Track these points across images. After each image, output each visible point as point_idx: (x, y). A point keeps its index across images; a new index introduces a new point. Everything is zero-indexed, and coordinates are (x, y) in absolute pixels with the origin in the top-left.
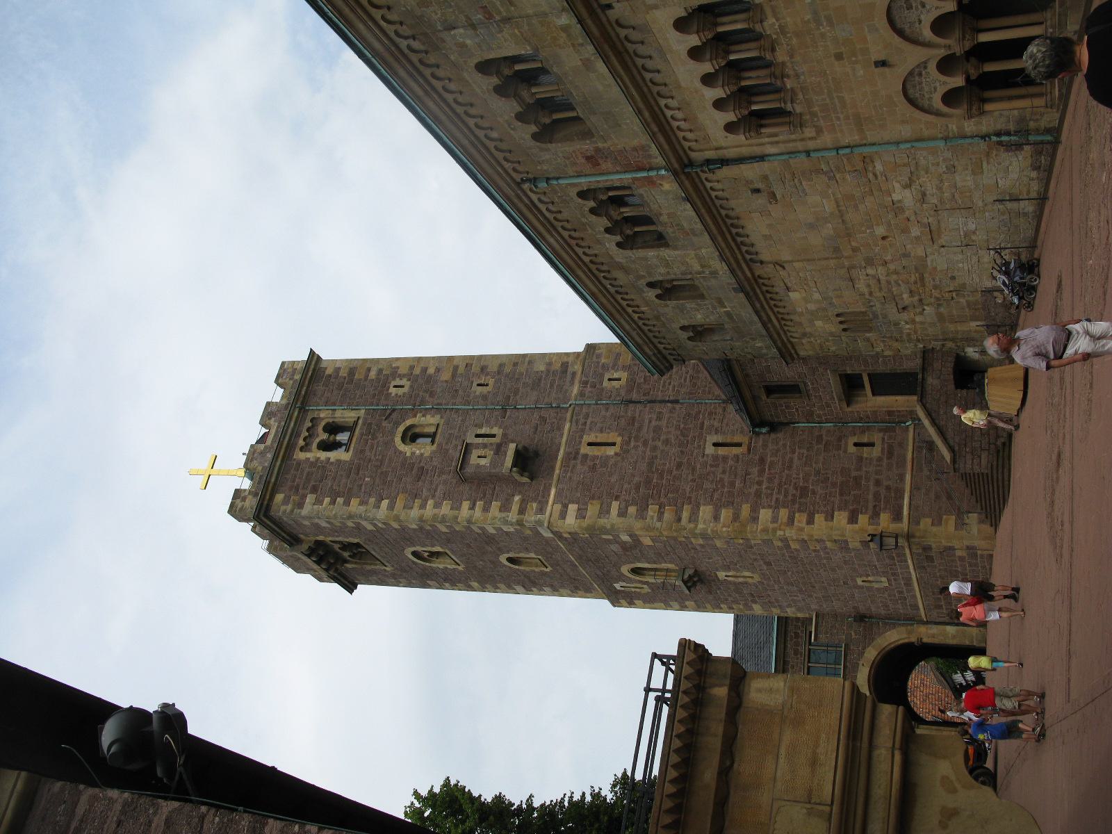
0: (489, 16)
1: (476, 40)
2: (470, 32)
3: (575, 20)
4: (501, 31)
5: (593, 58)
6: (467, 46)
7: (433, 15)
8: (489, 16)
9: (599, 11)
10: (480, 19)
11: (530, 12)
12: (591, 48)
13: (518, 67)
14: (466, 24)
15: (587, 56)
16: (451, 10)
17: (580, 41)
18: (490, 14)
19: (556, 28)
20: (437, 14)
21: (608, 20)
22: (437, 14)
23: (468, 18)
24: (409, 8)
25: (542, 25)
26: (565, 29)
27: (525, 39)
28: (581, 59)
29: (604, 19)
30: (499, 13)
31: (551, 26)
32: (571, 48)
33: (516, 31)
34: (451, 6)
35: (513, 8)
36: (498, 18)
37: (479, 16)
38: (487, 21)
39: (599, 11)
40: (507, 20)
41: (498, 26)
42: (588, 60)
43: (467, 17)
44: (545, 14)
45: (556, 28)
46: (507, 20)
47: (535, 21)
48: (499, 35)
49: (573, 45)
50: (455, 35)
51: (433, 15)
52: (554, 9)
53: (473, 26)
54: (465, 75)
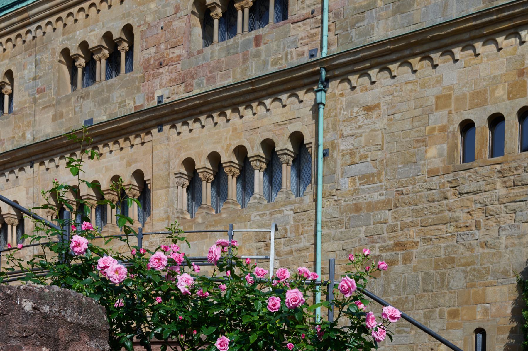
0: (39, 91)
1: (26, 78)
2: (32, 75)
3: (28, 143)
4: (29, 95)
5: (4, 147)
6: (24, 70)
7: (46, 56)
8: (39, 91)
9: (30, 159)
10: (38, 85)
11: (37, 118)
12: (10, 148)
13: (6, 97)
14: (37, 75)
15: (6, 144)
16: (47, 69)
17: (15, 143)
18: (41, 92)
19: (26, 130)
20: (46, 58)
21: (24, 163)
22: (46, 58)
23: (41, 77)
24: (53, 42)
25: (28, 123)
26: (24, 135)
27: (22, 108)
28: (4, 139)
29: (26, 161)
30: (40, 98)
31: (27, 128)
32: (12, 136)
33: (27, 105)
34: (49, 69)
35: (41, 108)
36: (37, 96)
37: (40, 85)
38: (36, 89)
39: (30, 159)
40: (35, 101)
41: (32, 95)
42: (3, 144)
43: (41, 77)
44: (34, 127)
45: (26, 130)
46: (35, 101)
47: (31, 119)
48: (27, 93)
49: (14, 137)
50: (32, 65)
51: (46, 56)
52: (36, 133)
53: (34, 79)
54: (7, 61)
